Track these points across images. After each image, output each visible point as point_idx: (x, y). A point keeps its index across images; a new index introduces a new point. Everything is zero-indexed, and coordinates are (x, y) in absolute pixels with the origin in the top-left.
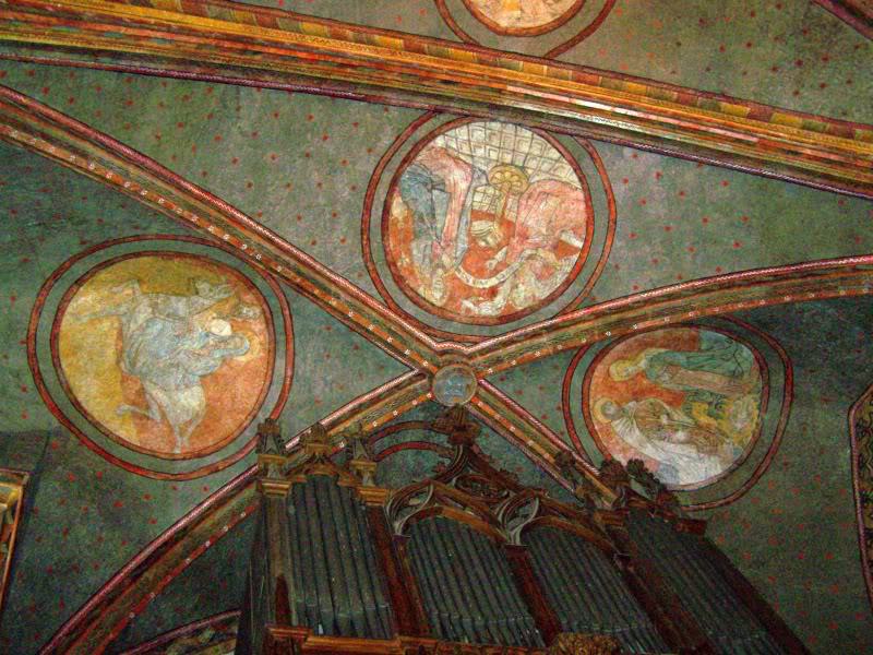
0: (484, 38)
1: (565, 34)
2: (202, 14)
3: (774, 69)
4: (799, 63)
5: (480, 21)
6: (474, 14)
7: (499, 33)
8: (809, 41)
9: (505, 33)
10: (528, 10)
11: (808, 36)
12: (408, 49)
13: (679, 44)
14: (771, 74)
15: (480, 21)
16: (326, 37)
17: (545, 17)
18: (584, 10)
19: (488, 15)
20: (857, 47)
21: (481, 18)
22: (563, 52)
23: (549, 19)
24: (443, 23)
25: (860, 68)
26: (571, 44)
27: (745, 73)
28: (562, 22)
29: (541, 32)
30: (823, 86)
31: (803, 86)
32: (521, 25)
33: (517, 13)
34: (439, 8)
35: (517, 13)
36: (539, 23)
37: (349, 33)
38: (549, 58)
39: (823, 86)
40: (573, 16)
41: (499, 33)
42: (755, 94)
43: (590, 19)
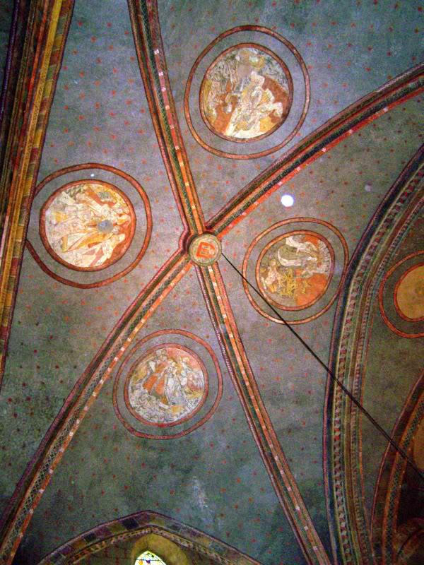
0: (39, 201)
1: (41, 253)
2: (61, 14)
3: (24, 385)
4: (28, 399)
5: (49, 199)
6: (54, 194)
7: (41, 210)
8: (42, 403)
9: (42, 214)
10: (56, 229)
11: (45, 402)
12: (33, 151)
13: (37, 325)
14: (21, 383)
15: (49, 199)
16: (43, 96)
17: (52, 239)
18: (57, 263)
19: (53, 203)
20: (39, 430)
21: (51, 199)
22: (30, 251)
23: (51, 242)
24: (48, 174)
25: (27, 435)
26: (36, 258)
27: (21, 367)
28: (49, 250)
29: (43, 237)
30: (15, 415)
31: (15, 404)
32: (47, 225)
33: (54, 222)
34: (59, 171)
35: (54, 222)
36: (48, 236)
37: (44, 113)
38: (26, 243)
39: (15, 415)
40: (53, 257)
41: (41, 210)
42: (8, 375)
43: (51, 267)
